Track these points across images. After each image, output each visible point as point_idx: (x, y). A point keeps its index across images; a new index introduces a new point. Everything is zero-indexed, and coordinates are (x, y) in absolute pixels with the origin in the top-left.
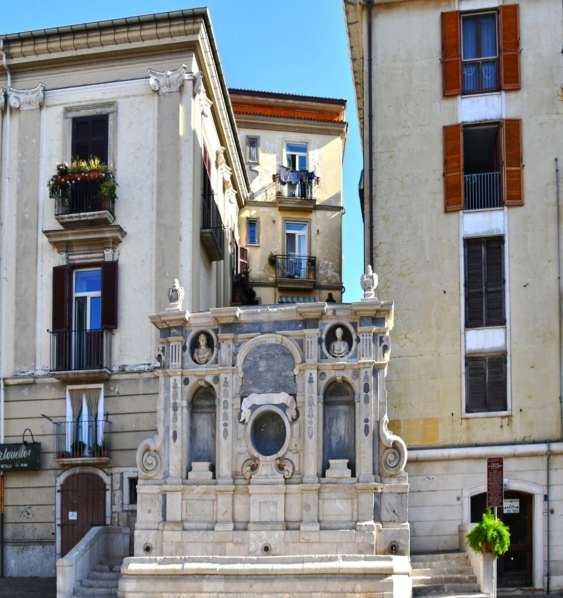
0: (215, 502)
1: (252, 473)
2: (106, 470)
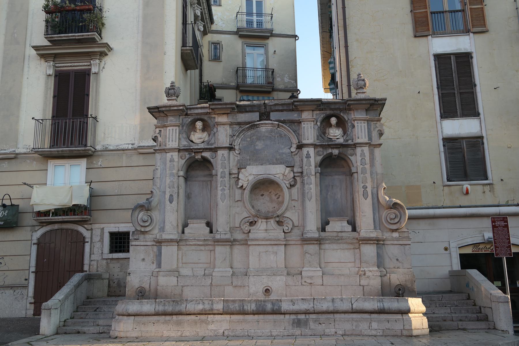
0: (212, 252)
2: (86, 226)
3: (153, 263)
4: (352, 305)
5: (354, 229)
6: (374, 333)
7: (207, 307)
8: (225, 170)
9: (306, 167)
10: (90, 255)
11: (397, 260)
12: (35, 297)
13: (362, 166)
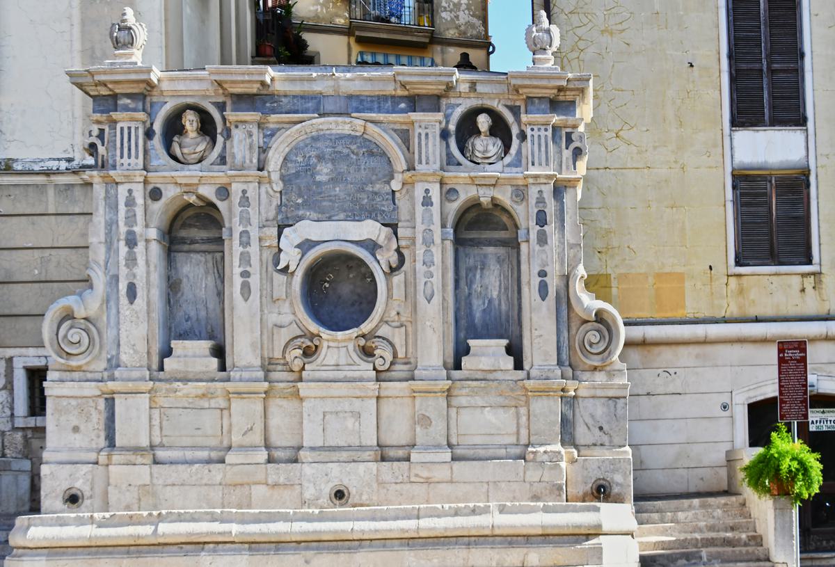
5: (518, 365)
8: (249, 228)
11: (601, 428)
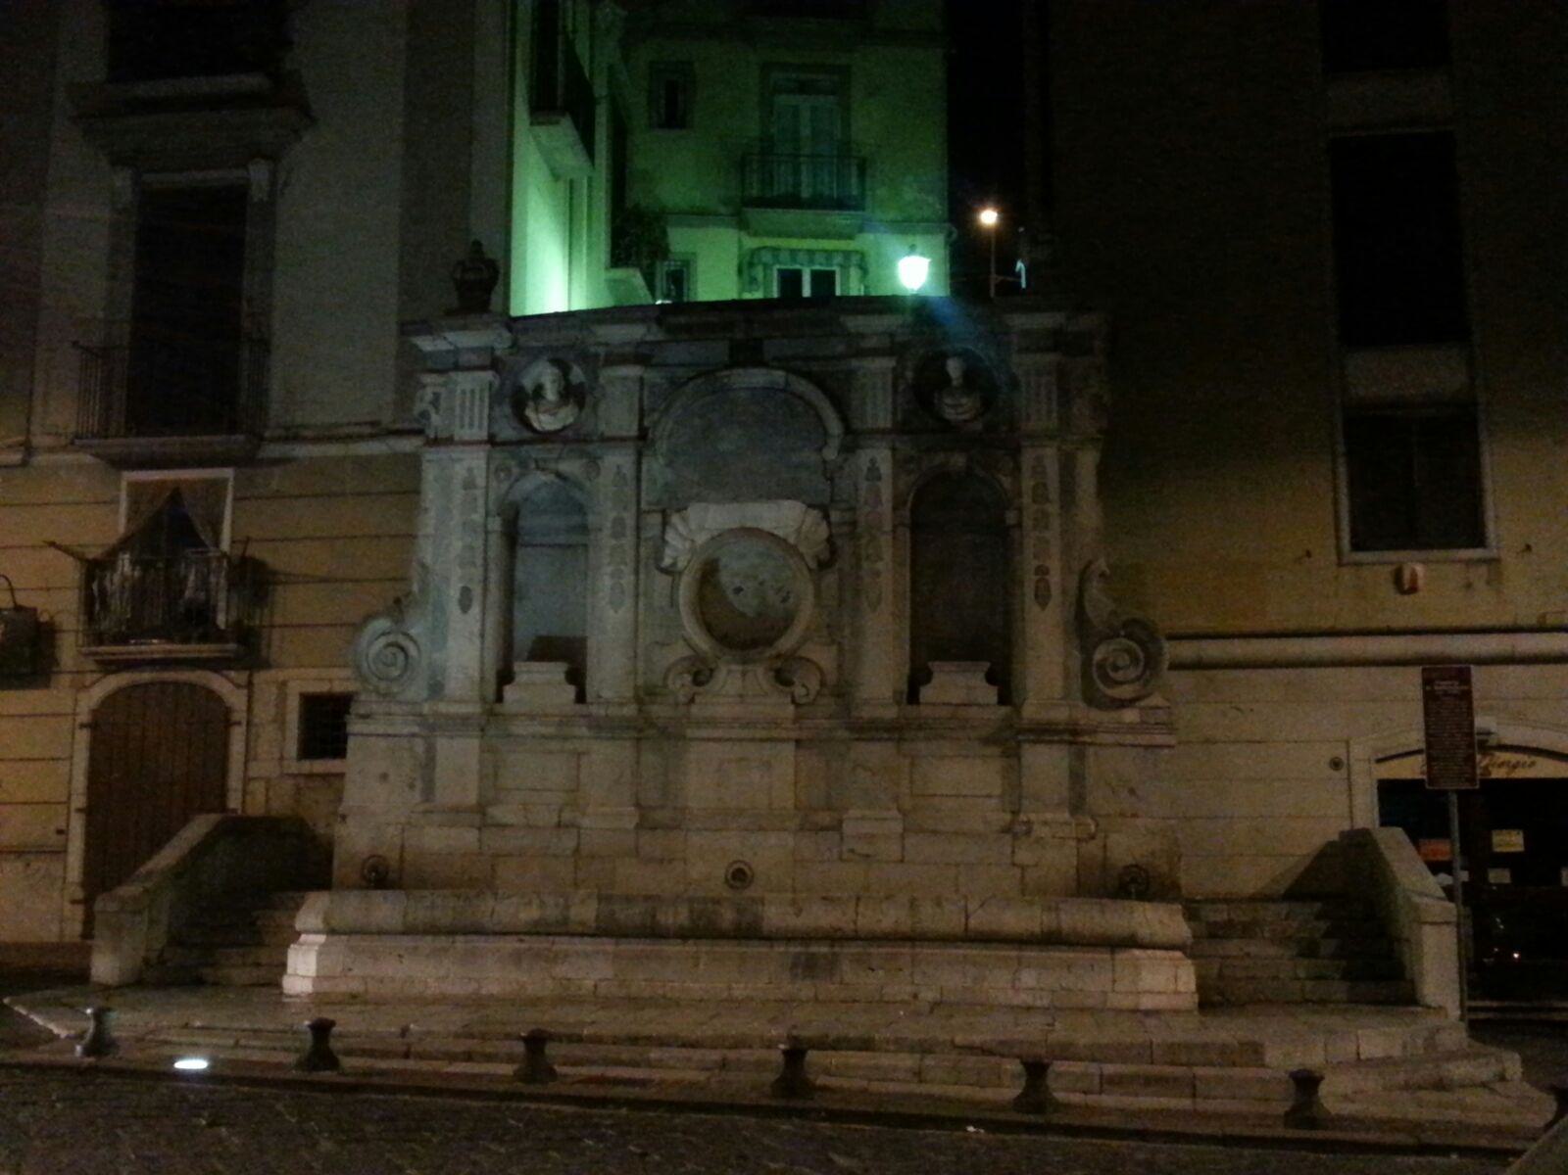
1: (696, 689)
2: (233, 674)
3: (412, 786)
4: (967, 917)
5: (1004, 699)
6: (1024, 998)
7: (552, 913)
9: (867, 509)
10: (246, 762)
12: (84, 885)
13: (1036, 507)
